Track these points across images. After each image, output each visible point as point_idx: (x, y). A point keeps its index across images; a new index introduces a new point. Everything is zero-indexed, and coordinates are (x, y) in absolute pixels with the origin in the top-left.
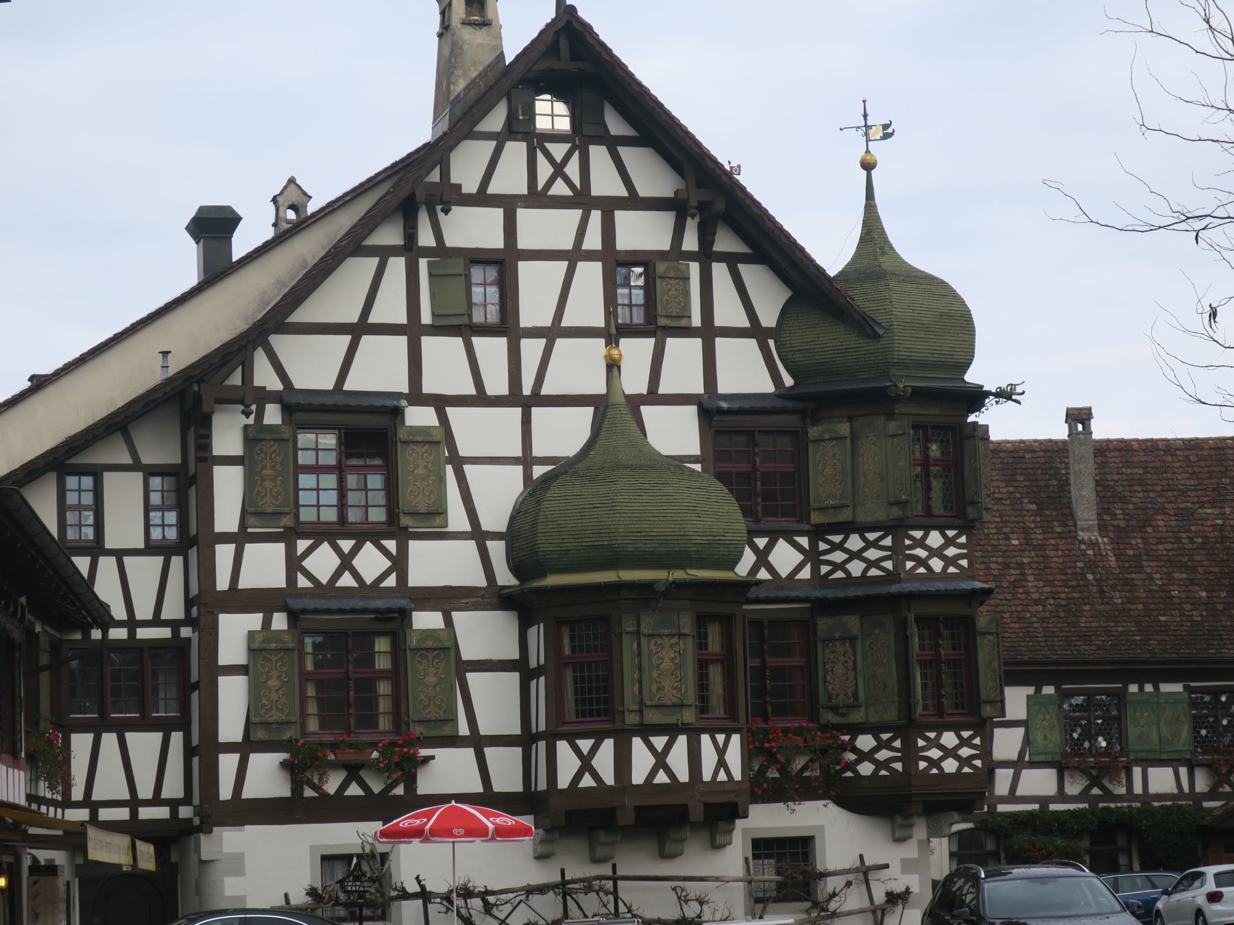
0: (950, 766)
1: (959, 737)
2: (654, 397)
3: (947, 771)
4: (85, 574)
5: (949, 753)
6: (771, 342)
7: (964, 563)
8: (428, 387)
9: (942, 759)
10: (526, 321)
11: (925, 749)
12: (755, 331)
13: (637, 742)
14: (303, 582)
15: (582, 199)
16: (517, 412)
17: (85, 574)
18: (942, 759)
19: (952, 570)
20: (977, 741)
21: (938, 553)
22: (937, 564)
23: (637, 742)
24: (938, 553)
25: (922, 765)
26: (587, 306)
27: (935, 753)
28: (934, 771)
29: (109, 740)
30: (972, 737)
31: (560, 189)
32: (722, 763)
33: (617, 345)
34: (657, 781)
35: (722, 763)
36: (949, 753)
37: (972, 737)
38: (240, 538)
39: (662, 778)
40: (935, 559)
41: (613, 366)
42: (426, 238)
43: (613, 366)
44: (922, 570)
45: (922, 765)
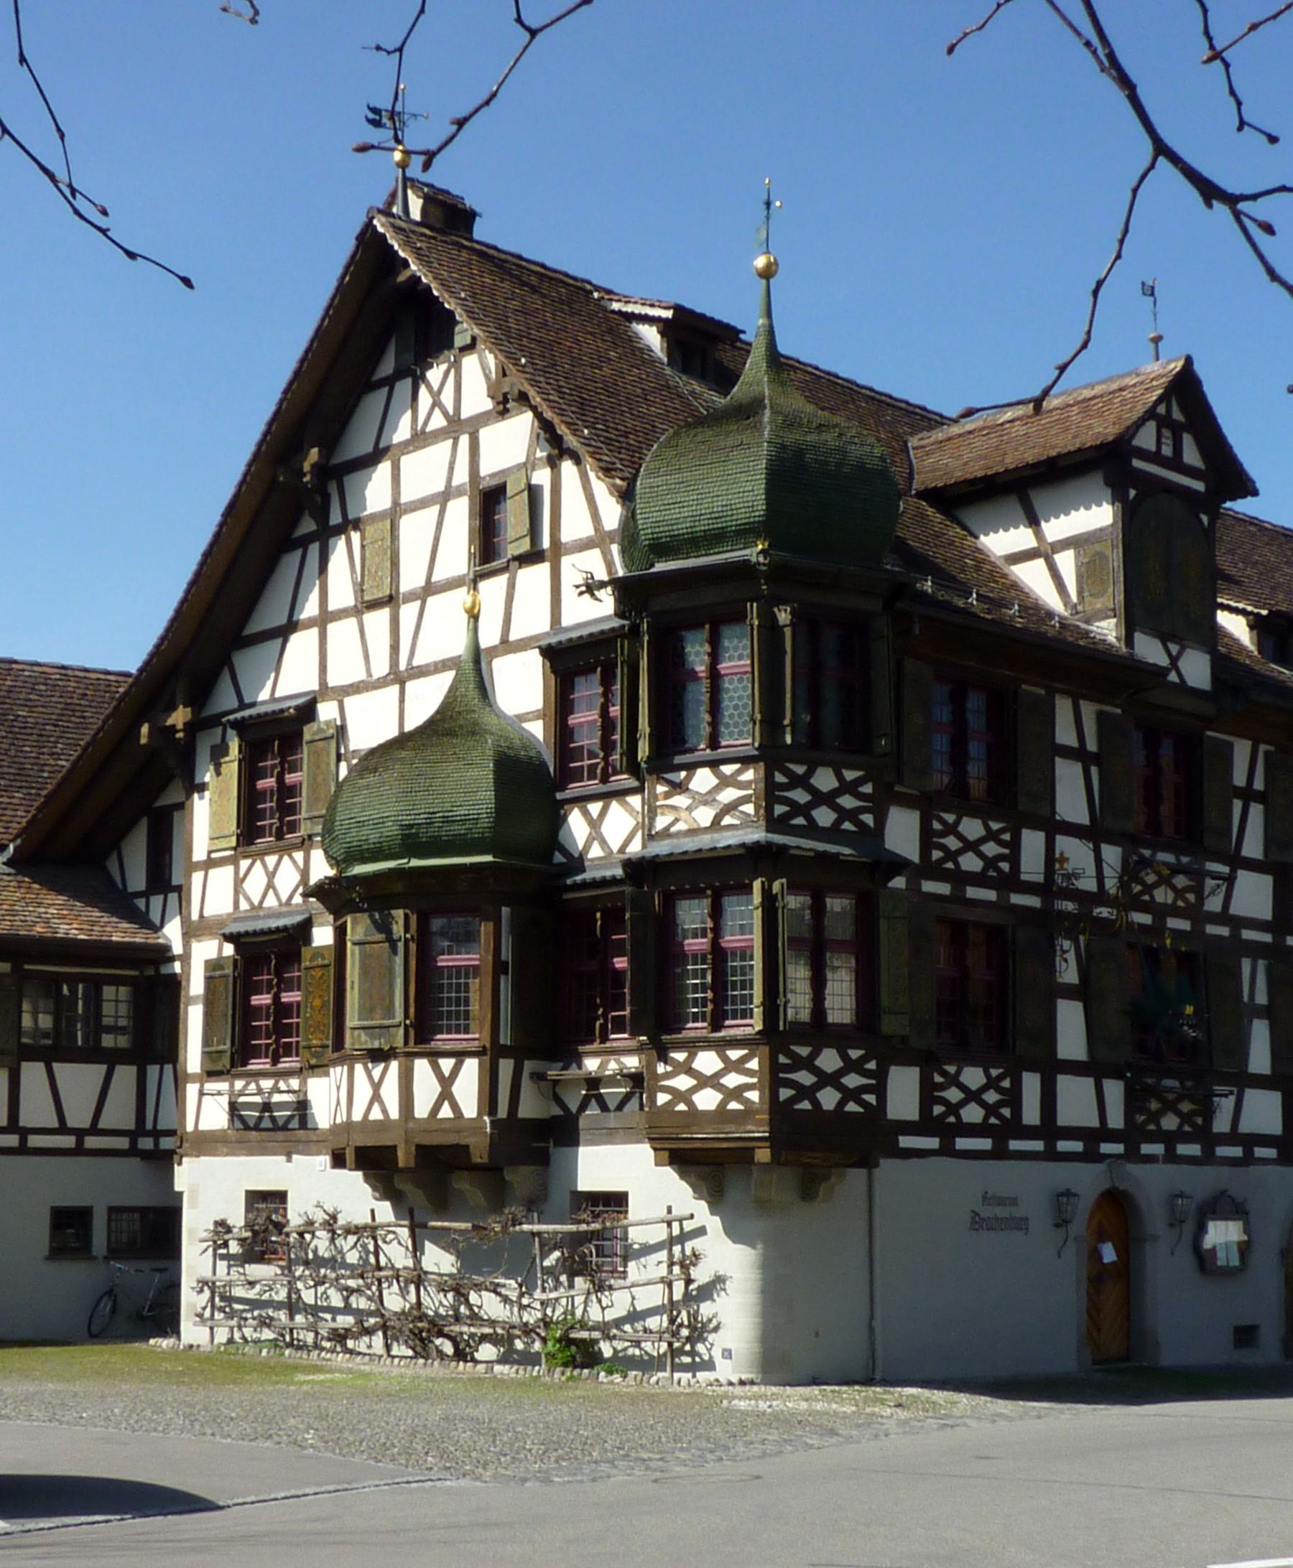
0: (707, 1100)
1: (844, 1056)
2: (507, 646)
3: (700, 1107)
4: (143, 909)
5: (705, 1082)
6: (615, 548)
8: (333, 681)
9: (694, 1090)
10: (404, 587)
11: (668, 1076)
12: (599, 540)
13: (359, 1068)
14: (244, 906)
15: (456, 426)
16: (395, 688)
17: (143, 909)
18: (694, 1090)
20: (754, 1064)
23: (359, 1068)
25: (662, 1098)
26: (457, 555)
27: (683, 1082)
28: (682, 1107)
29: (33, 1073)
30: (865, 1059)
31: (438, 421)
32: (376, 1097)
33: (475, 589)
34: (372, 1117)
35: (376, 1097)
36: (705, 1082)
37: (865, 1059)
38: (210, 864)
39: (376, 1114)
41: (474, 616)
42: (335, 518)
43: (474, 616)
45: (662, 1098)
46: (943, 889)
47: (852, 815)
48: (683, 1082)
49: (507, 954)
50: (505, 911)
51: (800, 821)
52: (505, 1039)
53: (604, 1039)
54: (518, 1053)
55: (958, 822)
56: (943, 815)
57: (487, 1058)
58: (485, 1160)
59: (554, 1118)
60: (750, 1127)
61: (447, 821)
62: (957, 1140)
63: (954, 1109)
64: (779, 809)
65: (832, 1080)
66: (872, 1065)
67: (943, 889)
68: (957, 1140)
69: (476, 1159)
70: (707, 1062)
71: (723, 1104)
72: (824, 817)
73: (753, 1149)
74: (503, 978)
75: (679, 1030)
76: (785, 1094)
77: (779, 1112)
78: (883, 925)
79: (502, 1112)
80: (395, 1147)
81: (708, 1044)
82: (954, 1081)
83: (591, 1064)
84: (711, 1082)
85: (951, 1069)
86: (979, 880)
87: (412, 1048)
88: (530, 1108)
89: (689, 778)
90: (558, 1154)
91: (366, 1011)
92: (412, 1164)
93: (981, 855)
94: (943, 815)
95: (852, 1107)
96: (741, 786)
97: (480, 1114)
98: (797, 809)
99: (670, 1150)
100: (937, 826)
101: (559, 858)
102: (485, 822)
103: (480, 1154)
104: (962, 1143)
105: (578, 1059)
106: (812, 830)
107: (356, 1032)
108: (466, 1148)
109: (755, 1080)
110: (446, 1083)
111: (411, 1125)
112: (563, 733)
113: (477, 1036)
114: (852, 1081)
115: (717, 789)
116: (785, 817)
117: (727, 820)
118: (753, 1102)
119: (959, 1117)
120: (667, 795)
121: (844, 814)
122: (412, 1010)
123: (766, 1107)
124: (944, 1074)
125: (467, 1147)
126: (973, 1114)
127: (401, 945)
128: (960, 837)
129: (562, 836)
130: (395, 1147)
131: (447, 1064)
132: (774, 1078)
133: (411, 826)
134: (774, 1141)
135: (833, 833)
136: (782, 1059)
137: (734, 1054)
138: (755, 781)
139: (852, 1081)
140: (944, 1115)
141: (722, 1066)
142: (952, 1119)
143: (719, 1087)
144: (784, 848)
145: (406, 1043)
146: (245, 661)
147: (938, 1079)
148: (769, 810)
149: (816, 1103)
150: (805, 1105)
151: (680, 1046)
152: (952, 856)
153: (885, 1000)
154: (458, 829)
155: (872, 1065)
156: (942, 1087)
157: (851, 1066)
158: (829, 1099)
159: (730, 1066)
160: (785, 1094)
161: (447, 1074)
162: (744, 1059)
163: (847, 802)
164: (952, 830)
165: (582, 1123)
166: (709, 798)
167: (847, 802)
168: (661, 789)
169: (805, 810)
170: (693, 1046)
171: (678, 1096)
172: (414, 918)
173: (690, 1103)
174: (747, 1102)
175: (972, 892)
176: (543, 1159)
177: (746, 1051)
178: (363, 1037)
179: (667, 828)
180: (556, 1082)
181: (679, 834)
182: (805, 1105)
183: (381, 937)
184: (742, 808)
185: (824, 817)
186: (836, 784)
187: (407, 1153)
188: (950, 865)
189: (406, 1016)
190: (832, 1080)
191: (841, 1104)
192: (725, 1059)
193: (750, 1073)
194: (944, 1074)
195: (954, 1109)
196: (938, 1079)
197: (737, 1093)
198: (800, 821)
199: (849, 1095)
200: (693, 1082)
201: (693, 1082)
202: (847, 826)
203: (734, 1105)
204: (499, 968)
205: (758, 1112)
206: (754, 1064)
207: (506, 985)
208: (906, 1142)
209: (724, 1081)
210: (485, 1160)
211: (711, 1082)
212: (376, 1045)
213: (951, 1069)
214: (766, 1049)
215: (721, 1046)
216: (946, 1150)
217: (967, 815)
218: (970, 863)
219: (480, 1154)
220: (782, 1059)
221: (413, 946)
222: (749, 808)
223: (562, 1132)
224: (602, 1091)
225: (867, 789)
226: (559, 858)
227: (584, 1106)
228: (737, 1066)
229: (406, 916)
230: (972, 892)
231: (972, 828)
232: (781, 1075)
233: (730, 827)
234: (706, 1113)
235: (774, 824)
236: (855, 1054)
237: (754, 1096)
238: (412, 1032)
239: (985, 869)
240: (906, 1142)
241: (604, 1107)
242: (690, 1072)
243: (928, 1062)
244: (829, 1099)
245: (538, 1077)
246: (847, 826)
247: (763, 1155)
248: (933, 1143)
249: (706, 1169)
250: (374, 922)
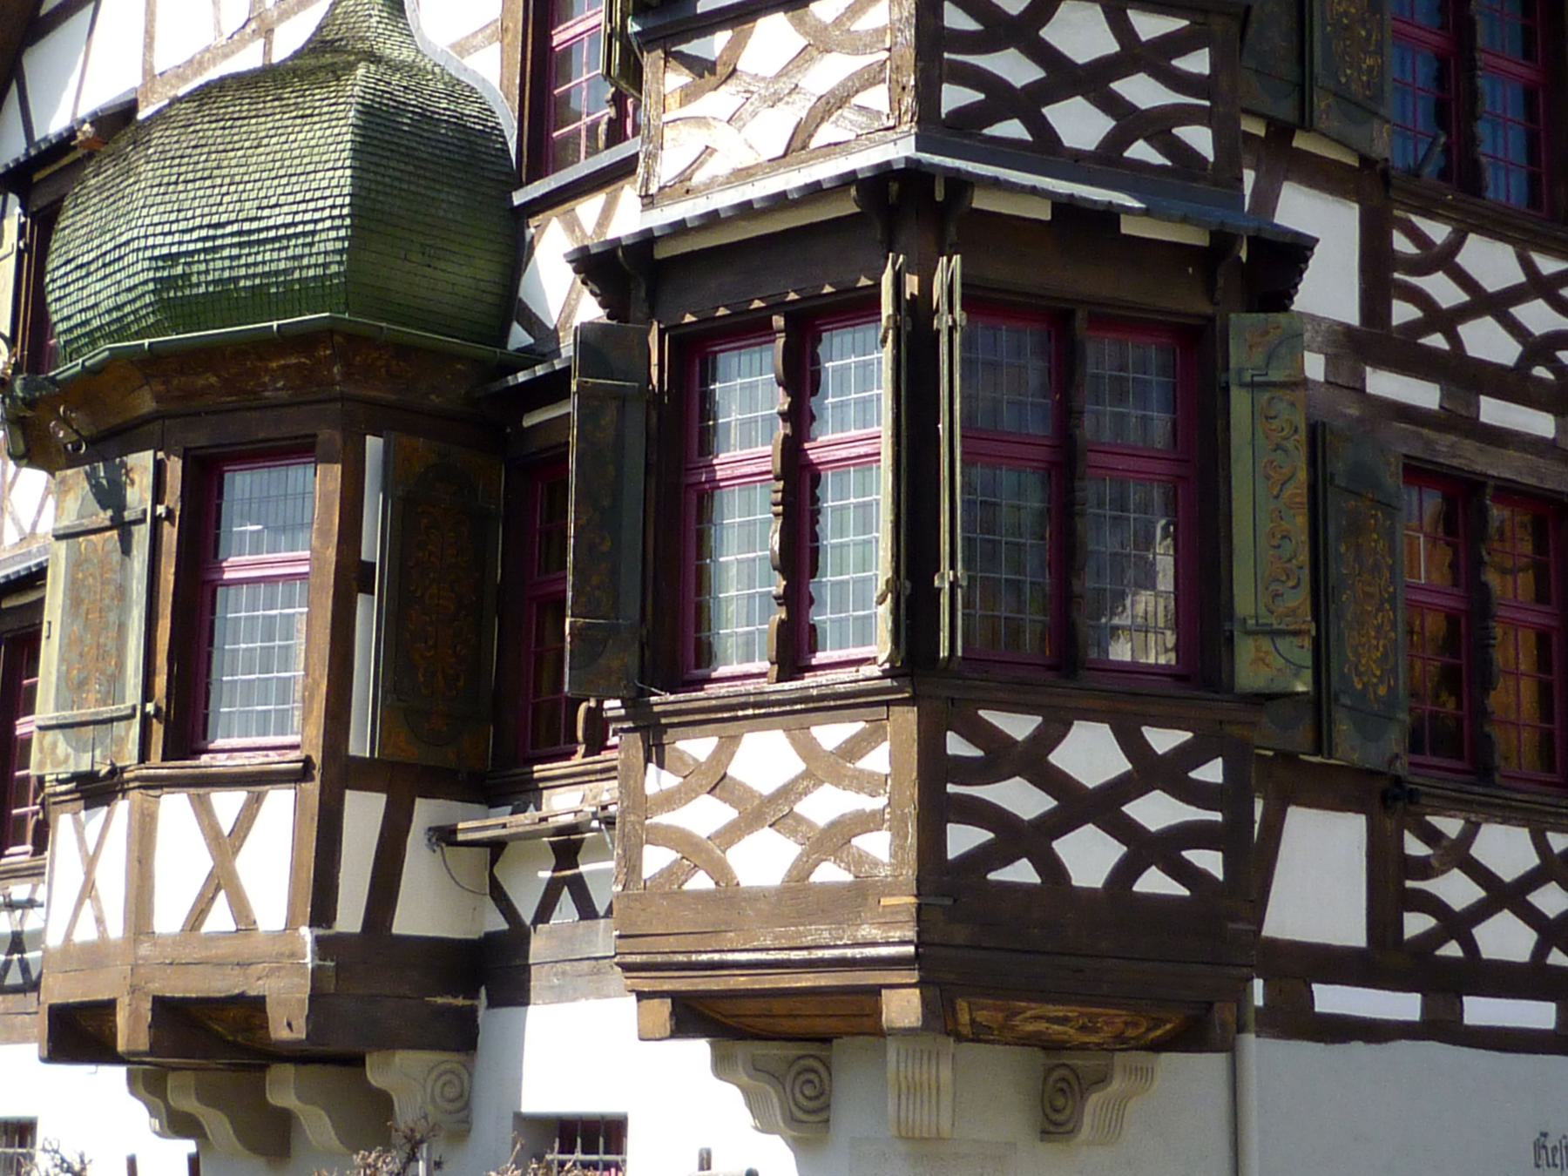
0: (763, 861)
7: (877, 97)
9: (730, 834)
11: (670, 800)
18: (730, 834)
20: (878, 760)
25: (655, 859)
27: (704, 816)
28: (701, 882)
40: (766, 114)
45: (655, 859)
46: (1424, 394)
47: (1157, 125)
48: (704, 816)
49: (371, 548)
50: (374, 444)
51: (1012, 129)
52: (359, 745)
53: (597, 744)
54: (400, 779)
55: (1455, 244)
56: (1417, 220)
57: (313, 788)
58: (300, 1033)
59: (491, 938)
60: (867, 931)
61: (248, 241)
62: (1468, 1001)
64: (954, 97)
65: (1100, 807)
66: (1212, 772)
67: (1424, 394)
68: (1468, 1001)
69: (280, 1032)
70: (764, 757)
71: (800, 871)
72: (1079, 124)
73: (876, 991)
74: (361, 598)
75: (699, 684)
76: (962, 839)
77: (943, 886)
78: (1240, 403)
79: (350, 917)
80: (109, 1006)
81: (763, 711)
82: (1459, 856)
83: (563, 803)
84: (770, 811)
85: (1451, 826)
86: (1510, 384)
87: (157, 766)
88: (424, 910)
89: (736, 47)
90: (491, 1020)
91: (73, 687)
92: (143, 1043)
93: (1516, 329)
94: (1417, 220)
95: (1154, 882)
96: (856, 45)
97: (291, 924)
98: (1002, 100)
99: (677, 998)
100: (1402, 244)
101: (519, 337)
102: (331, 239)
103: (288, 1022)
104: (1479, 1011)
105: (525, 793)
106: (1045, 150)
107: (50, 735)
108: (257, 1004)
110: (226, 846)
111: (145, 949)
112: (542, 69)
113: (301, 735)
114: (1156, 811)
115: (802, 59)
116: (968, 120)
117: (826, 134)
118: (876, 864)
119: (1470, 946)
120: (688, 95)
121: (1131, 122)
122: (161, 682)
123: (909, 873)
124: (1431, 836)
125: (258, 1003)
126: (1505, 938)
127: (142, 534)
128: (1463, 279)
129: (525, 292)
130: (109, 1006)
131: (228, 804)
132: (936, 797)
133: (172, 258)
134: (933, 964)
135: (1106, 162)
136: (956, 745)
137: (831, 734)
138: (893, 28)
139: (1156, 811)
140: (1432, 939)
141: (797, 766)
142: (1452, 949)
143: (787, 823)
144: (961, 184)
145: (144, 756)
146: (39, 62)
147: (1415, 847)
148: (927, 96)
149: (1052, 869)
150: (1022, 872)
151: (700, 720)
152: (1447, 321)
153: (1245, 601)
154: (271, 259)
155: (1212, 772)
156: (1424, 869)
157: (1150, 772)
158: (1089, 857)
160: (962, 839)
161: (226, 828)
162: (853, 749)
163: (1142, 91)
164: (1442, 259)
165: (540, 946)
166: (784, 86)
167: (1142, 91)
168: (677, 79)
169: (1028, 103)
170: (733, 716)
171: (693, 851)
172: (175, 467)
173: (720, 871)
174: (859, 861)
175: (1494, 411)
176: (461, 1036)
177: (861, 725)
178: (63, 748)
179: (684, 177)
180: (496, 848)
181: (709, 187)
182: (1022, 872)
183: (104, 517)
184: (859, 99)
185: (1079, 124)
186: (1113, 47)
187: (134, 1015)
188: (1437, 341)
189: (147, 695)
190: (1100, 807)
191: (1126, 872)
192: (807, 750)
193: (865, 782)
194: (1431, 836)
195: (1459, 924)
196: (1415, 847)
197: (835, 839)
198: (1012, 129)
199: (1146, 848)
202: (1140, 151)
203: (829, 873)
204: (351, 577)
205: (890, 889)
206: (878, 760)
207: (367, 612)
208: (1330, 999)
209: (804, 808)
210: (300, 1033)
211: (770, 811)
212: (85, 767)
213: (1451, 826)
214: (906, 719)
216: (1442, 1026)
217: (1482, 230)
218: (1487, 341)
219: (288, 1022)
220: (956, 745)
221: (170, 534)
222: (877, 97)
223: (490, 972)
224: (583, 869)
225: (1197, 63)
226: (519, 337)
227: (544, 912)
229: (159, 468)
230: (1494, 411)
231: (1492, 262)
232: (951, 788)
233: (833, 147)
234: (757, 896)
235: (934, 127)
236: (1163, 740)
237: (876, 844)
238: (158, 730)
239: (1526, 361)
240: (1330, 999)
241: (587, 910)
242: (720, 784)
243: (1386, 801)
244: (1089, 857)
245: (444, 836)
246: (1140, 151)
247: (903, 1007)
248: (1406, 1006)
249: (774, 1050)
250: (97, 489)
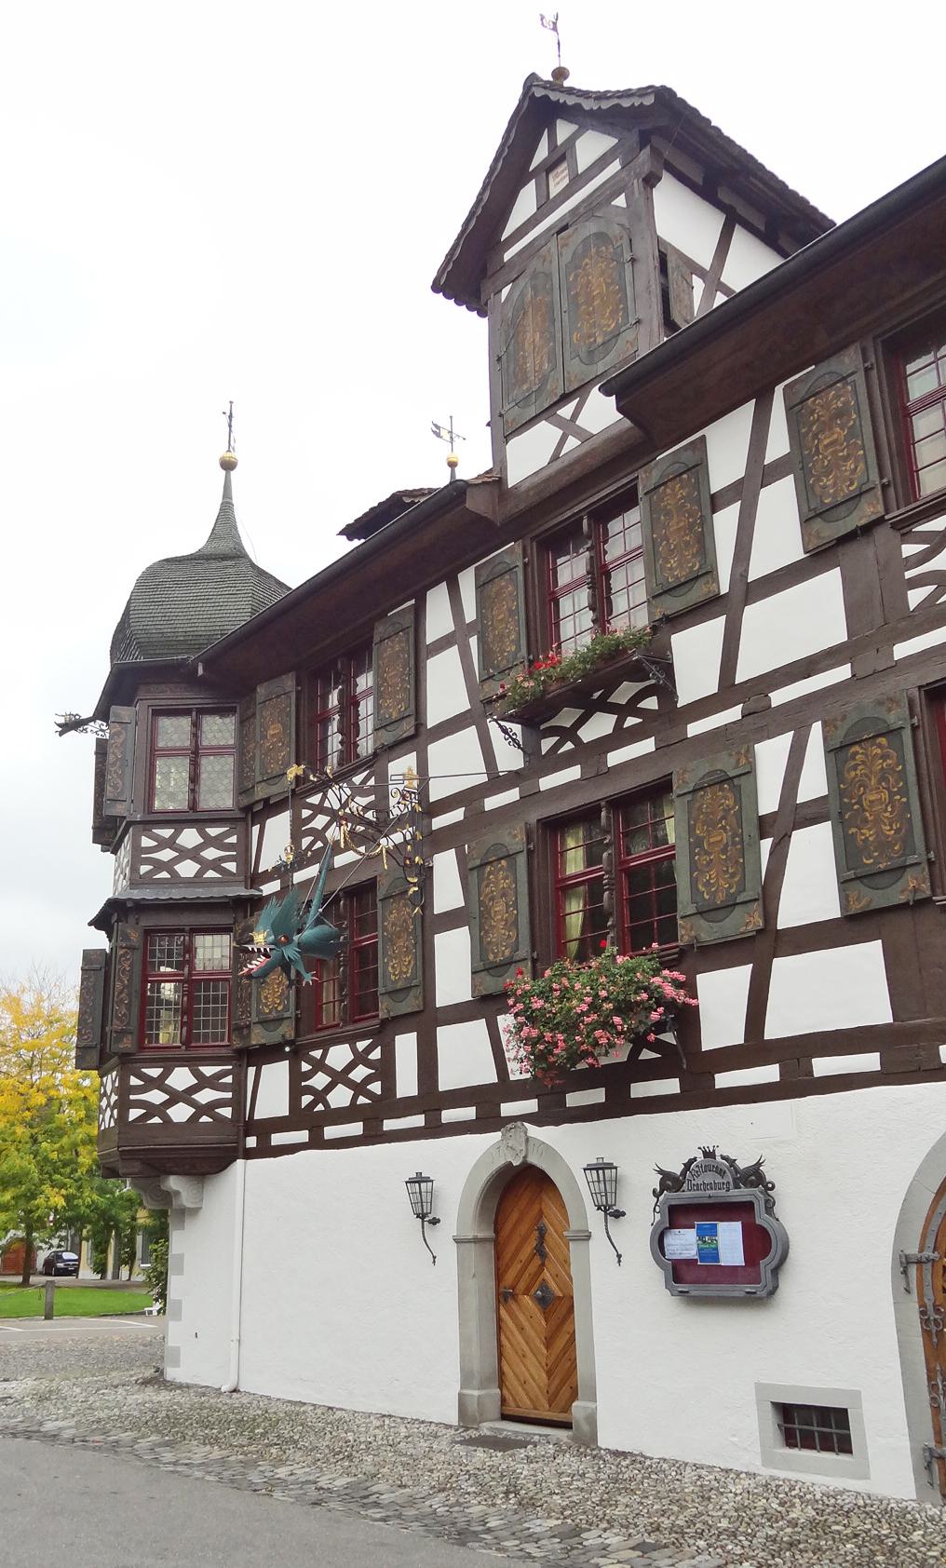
19: (211, 874)
21: (194, 854)
22: (187, 869)
24: (194, 854)
27: (156, 1097)
28: (156, 1120)
44: (164, 875)
45: (134, 1114)
63: (320, 1096)
70: (181, 1078)
71: (194, 1118)
81: (182, 1062)
82: (320, 1066)
84: (186, 1096)
104: (331, 1132)
109: (229, 1095)
119: (326, 1104)
137: (208, 1071)
142: (320, 1107)
151: (153, 1063)
156: (309, 1075)
159: (203, 1083)
170: (169, 1063)
171: (152, 1110)
192: (197, 1074)
193: (223, 1088)
195: (320, 1096)
197: (210, 1108)
200: (164, 1097)
201: (164, 1097)
215: (192, 1063)
228: (212, 1083)
